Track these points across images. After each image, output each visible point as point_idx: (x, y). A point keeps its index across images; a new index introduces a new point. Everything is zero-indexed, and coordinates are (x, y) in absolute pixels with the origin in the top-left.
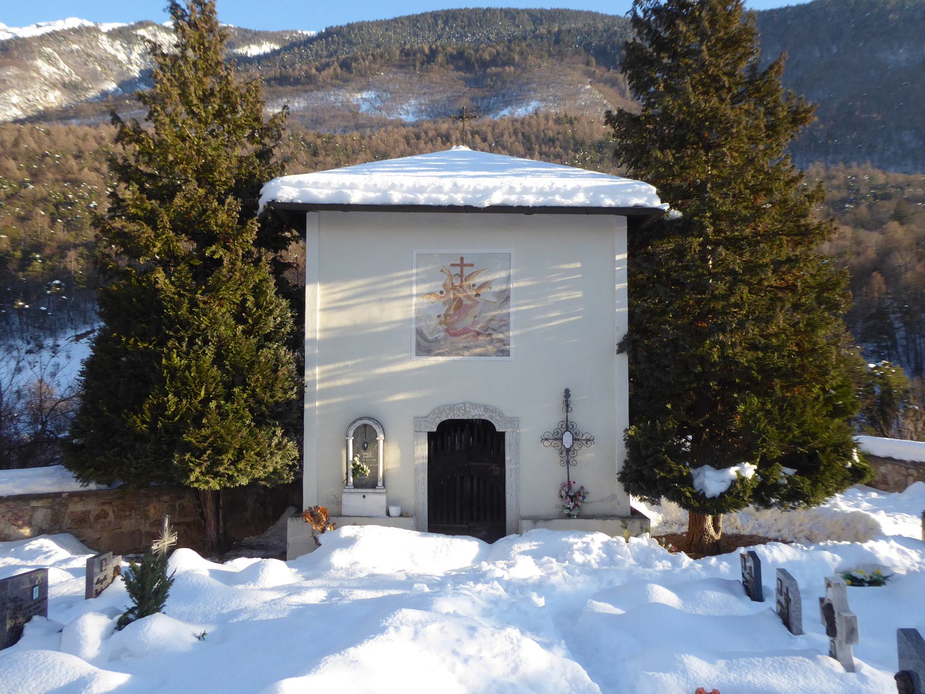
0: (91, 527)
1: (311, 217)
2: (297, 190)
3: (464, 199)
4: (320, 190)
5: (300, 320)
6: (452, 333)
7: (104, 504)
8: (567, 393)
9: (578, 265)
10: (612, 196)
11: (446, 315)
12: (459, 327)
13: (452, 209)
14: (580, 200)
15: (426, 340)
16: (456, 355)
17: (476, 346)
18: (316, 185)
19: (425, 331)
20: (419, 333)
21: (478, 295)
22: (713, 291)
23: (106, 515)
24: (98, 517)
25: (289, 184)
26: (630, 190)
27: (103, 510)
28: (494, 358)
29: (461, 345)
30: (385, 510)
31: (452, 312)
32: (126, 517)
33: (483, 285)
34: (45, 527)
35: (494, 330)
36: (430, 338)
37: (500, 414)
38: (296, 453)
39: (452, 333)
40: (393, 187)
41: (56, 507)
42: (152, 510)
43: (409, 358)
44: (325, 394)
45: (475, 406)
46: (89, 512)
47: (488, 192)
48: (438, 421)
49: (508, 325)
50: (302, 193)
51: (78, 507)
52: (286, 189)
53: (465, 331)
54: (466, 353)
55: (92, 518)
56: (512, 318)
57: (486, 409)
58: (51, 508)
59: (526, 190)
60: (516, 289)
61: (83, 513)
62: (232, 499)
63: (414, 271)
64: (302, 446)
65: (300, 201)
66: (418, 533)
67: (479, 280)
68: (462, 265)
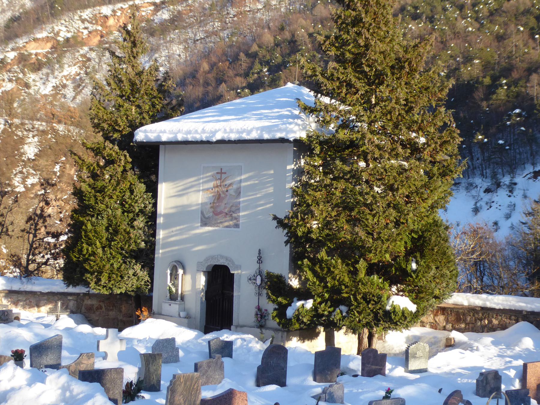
0: (94, 313)
1: (162, 148)
2: (144, 134)
3: (206, 137)
4: (152, 134)
5: (155, 205)
6: (216, 214)
7: (100, 301)
8: (260, 250)
9: (272, 172)
10: (269, 132)
11: (213, 203)
12: (219, 210)
13: (202, 142)
14: (254, 135)
15: (205, 217)
16: (217, 227)
17: (225, 221)
18: (151, 131)
19: (204, 212)
20: (202, 213)
21: (227, 191)
22: (37, 215)
23: (101, 308)
24: (97, 309)
25: (141, 131)
26: (276, 129)
27: (99, 305)
28: (233, 229)
29: (219, 221)
30: (178, 313)
31: (216, 201)
32: (112, 310)
33: (230, 185)
34: (74, 310)
35: (233, 212)
36: (206, 216)
37: (233, 262)
38: (147, 278)
39: (216, 214)
40: (179, 131)
41: (79, 301)
42: (124, 308)
43: (197, 228)
44: (165, 246)
45: (222, 257)
46: (93, 305)
47: (214, 133)
48: (206, 265)
49: (239, 209)
50: (146, 136)
51: (88, 302)
52: (143, 134)
53: (221, 213)
54: (221, 226)
55: (95, 308)
56: (241, 205)
57: (227, 259)
58: (77, 301)
59: (231, 131)
60: (245, 186)
61: (90, 305)
62: (112, 300)
63: (202, 176)
64: (153, 274)
65: (145, 141)
66: (176, 325)
67: (228, 182)
68: (221, 173)
